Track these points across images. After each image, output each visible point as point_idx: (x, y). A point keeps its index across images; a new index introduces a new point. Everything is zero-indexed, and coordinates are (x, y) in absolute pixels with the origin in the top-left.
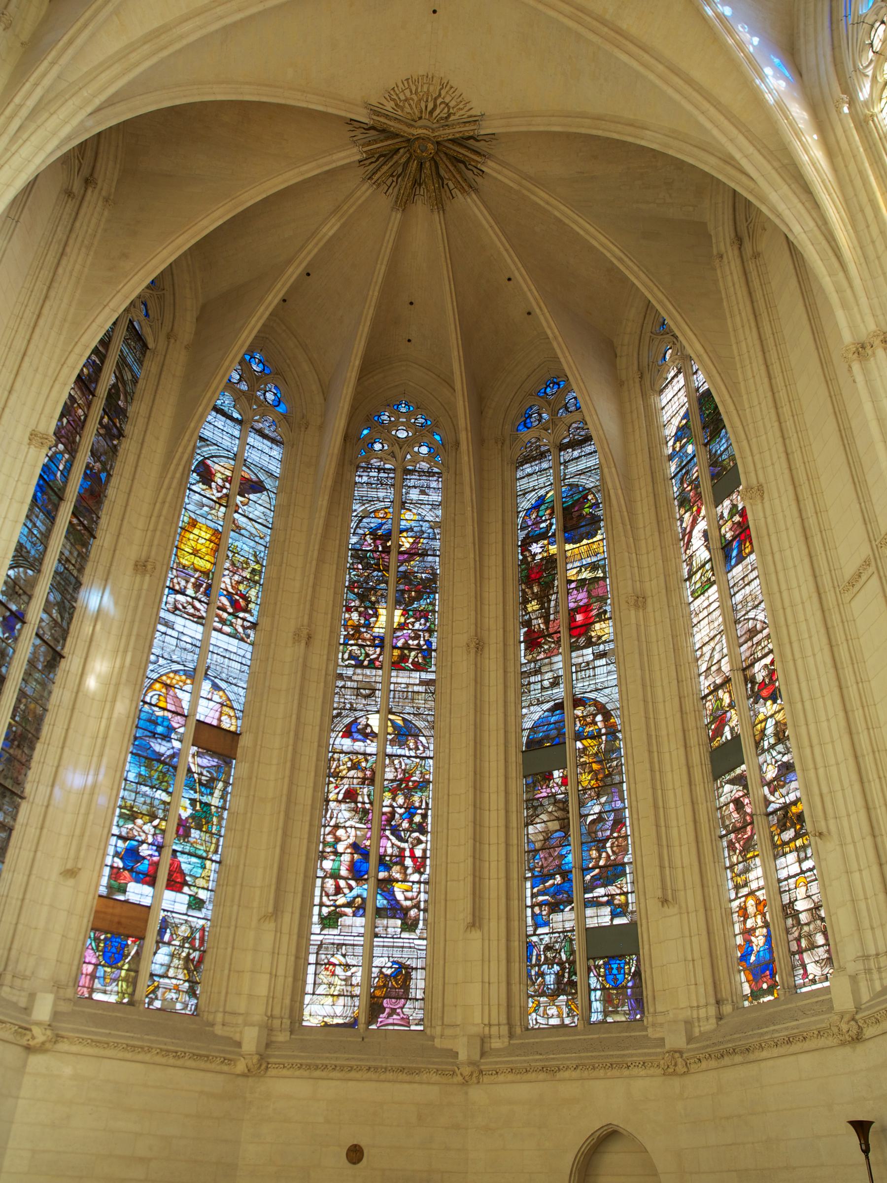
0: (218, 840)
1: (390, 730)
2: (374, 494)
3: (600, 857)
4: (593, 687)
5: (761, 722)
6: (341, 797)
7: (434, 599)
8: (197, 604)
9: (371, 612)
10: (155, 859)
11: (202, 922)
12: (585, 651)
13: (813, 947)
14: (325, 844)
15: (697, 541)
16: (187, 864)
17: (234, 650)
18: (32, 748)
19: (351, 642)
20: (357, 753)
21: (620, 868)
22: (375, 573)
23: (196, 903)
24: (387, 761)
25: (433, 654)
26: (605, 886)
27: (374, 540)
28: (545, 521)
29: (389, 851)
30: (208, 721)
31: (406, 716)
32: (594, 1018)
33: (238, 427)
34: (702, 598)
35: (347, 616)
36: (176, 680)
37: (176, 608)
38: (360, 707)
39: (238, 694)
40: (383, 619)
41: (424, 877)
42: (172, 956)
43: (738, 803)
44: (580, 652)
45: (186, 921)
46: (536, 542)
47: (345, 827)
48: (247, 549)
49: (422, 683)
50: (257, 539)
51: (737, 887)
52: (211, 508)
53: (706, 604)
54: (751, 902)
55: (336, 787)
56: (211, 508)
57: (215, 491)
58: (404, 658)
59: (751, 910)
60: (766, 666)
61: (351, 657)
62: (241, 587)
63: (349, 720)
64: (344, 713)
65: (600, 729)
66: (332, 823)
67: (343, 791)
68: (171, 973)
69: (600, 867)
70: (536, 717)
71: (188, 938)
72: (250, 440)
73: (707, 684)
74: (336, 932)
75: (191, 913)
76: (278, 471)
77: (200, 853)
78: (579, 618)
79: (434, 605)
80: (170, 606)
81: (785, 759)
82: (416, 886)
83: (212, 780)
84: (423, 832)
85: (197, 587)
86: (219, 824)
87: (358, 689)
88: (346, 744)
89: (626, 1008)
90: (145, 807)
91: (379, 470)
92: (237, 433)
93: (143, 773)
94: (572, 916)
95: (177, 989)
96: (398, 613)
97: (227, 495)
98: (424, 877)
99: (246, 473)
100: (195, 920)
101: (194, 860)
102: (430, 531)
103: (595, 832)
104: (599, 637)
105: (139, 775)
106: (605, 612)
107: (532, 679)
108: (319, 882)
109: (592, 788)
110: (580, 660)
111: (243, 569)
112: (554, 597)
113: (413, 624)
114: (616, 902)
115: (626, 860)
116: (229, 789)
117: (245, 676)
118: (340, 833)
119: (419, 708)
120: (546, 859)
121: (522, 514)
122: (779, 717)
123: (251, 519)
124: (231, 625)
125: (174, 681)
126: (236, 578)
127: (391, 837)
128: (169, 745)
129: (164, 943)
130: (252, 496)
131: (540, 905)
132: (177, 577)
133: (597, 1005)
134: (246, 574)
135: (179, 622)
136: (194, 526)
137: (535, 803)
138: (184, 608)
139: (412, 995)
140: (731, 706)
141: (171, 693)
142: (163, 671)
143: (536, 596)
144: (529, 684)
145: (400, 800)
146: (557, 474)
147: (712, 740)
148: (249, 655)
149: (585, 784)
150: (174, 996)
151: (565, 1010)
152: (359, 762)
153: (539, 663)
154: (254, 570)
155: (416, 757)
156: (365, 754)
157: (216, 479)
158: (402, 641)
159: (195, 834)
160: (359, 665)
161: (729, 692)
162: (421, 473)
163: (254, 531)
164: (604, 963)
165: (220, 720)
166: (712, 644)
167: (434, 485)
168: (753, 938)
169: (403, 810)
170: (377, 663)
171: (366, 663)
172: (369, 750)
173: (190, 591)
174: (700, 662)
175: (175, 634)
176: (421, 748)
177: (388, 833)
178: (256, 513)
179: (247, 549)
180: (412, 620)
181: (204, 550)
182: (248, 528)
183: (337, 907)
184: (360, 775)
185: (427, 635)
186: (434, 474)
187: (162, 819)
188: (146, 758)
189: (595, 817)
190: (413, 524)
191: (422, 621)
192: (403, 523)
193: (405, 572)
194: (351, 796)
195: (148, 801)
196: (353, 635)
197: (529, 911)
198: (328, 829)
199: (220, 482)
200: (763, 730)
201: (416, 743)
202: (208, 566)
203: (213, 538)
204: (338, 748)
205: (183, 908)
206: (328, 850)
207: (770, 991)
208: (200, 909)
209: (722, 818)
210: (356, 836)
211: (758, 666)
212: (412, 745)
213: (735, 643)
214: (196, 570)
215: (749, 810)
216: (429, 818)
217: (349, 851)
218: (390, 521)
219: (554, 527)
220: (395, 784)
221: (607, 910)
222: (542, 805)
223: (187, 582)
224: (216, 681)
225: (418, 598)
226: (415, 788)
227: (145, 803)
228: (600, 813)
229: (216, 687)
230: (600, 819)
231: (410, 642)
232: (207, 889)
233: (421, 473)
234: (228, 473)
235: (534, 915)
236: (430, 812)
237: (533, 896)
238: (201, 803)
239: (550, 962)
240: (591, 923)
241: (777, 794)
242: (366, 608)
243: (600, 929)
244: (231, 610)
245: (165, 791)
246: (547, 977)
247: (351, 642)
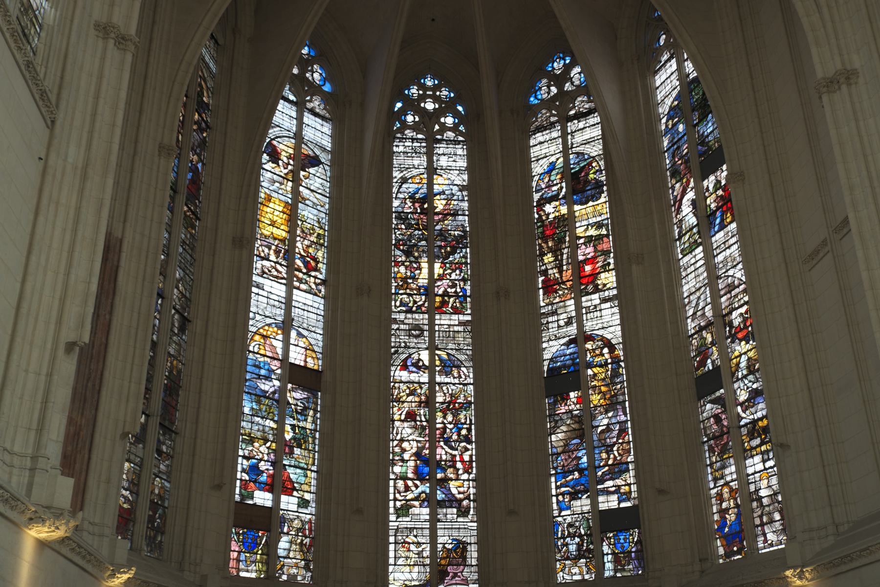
0: (314, 455)
1: (438, 363)
2: (409, 162)
3: (609, 458)
4: (600, 326)
5: (736, 357)
6: (403, 417)
7: (466, 253)
8: (278, 267)
9: (415, 265)
10: (271, 472)
11: (309, 517)
12: (594, 296)
13: (771, 521)
14: (393, 453)
15: (686, 208)
16: (294, 474)
17: (310, 303)
18: (178, 395)
19: (401, 292)
20: (413, 382)
21: (625, 466)
22: (416, 232)
24: (437, 388)
25: (468, 299)
26: (612, 479)
27: (413, 203)
28: (557, 184)
29: (444, 457)
30: (297, 362)
31: (450, 351)
32: (607, 574)
33: (294, 108)
34: (690, 256)
35: (396, 269)
36: (271, 331)
37: (264, 272)
38: (412, 345)
39: (317, 339)
40: (425, 272)
41: (472, 476)
42: (291, 542)
43: (717, 418)
44: (589, 297)
46: (550, 203)
47: (408, 441)
48: (312, 217)
49: (461, 324)
50: (319, 207)
51: (715, 480)
52: (281, 184)
53: (693, 261)
54: (726, 490)
55: (399, 409)
56: (281, 184)
57: (282, 168)
58: (444, 303)
59: (726, 496)
60: (741, 314)
61: (402, 304)
62: (311, 250)
63: (404, 356)
64: (400, 350)
65: (607, 360)
66: (398, 437)
67: (404, 413)
69: (609, 465)
70: (554, 350)
71: (300, 529)
72: (305, 120)
73: (693, 325)
74: (408, 519)
75: (300, 510)
76: (330, 145)
77: (302, 465)
78: (588, 268)
79: (466, 258)
80: (259, 271)
81: (755, 386)
82: (466, 483)
83: (305, 408)
84: (469, 442)
85: (277, 253)
86: (314, 443)
87: (410, 330)
88: (404, 375)
89: (631, 567)
90: (259, 433)
91: (413, 140)
92: (294, 114)
93: (255, 407)
94: (588, 502)
95: (297, 567)
96: (437, 266)
97: (291, 171)
98: (472, 476)
99: (305, 150)
101: (298, 471)
102: (459, 193)
103: (605, 439)
104: (605, 285)
105: (252, 409)
106: (609, 264)
107: (550, 319)
108: (392, 483)
109: (601, 405)
110: (589, 304)
111: (311, 234)
112: (565, 251)
113: (450, 275)
114: (622, 491)
115: (629, 460)
116: (318, 415)
117: (321, 325)
118: (405, 445)
119: (459, 344)
120: (566, 460)
121: (536, 178)
122: (751, 354)
123: (312, 191)
124: (306, 282)
125: (269, 333)
126: (306, 242)
127: (445, 447)
128: (271, 384)
130: (312, 170)
131: (563, 494)
132: (261, 245)
133: (609, 565)
134: (313, 238)
135: (267, 283)
136: (270, 201)
137: (557, 418)
138: (270, 271)
139: (469, 561)
140: (713, 344)
141: (268, 342)
142: (260, 325)
143: (551, 250)
144: (548, 323)
145: (450, 418)
146: (565, 143)
147: (697, 369)
148: (322, 307)
149: (595, 402)
150: (296, 571)
151: (585, 569)
152: (415, 390)
153: (555, 306)
154: (319, 235)
155: (460, 384)
156: (419, 383)
157: (282, 157)
158: (443, 289)
159: (297, 451)
160: (409, 311)
161: (712, 333)
162: (449, 142)
163: (315, 201)
164: (614, 536)
165: (305, 361)
166: (698, 294)
167: (460, 152)
168: (727, 516)
169: (452, 426)
170: (423, 309)
171: (414, 309)
172: (422, 380)
173: (273, 257)
174: (687, 308)
175: (265, 294)
176: (463, 377)
177: (442, 444)
178: (317, 185)
179: (312, 217)
180: (449, 271)
181: (279, 221)
182: (311, 198)
183: (407, 501)
184: (417, 399)
185: (462, 284)
186: (459, 142)
187: (272, 442)
188: (256, 395)
189: (604, 427)
190: (445, 188)
191: (458, 272)
192: (436, 187)
193: (441, 230)
194: (411, 416)
195: (261, 428)
196: (402, 286)
197: (554, 499)
198: (395, 443)
199: (285, 160)
200: (738, 364)
201: (459, 372)
202: (284, 234)
203: (285, 210)
204: (398, 378)
205: (295, 508)
206: (397, 458)
207: (738, 552)
208: (306, 508)
209: (705, 428)
210: (418, 447)
211: (735, 314)
212: (456, 375)
213: (716, 296)
214: (275, 239)
215: (725, 423)
216: (473, 431)
217: (413, 458)
218: (425, 186)
219: (564, 190)
220: (445, 406)
221: (615, 497)
222: (561, 419)
223: (270, 249)
224: (300, 330)
225: (453, 252)
226: (461, 408)
227: (258, 430)
228: (608, 425)
229: (300, 335)
230: (608, 429)
231: (449, 290)
232: (310, 492)
233: (449, 142)
234: (291, 151)
235: (558, 502)
236: (473, 427)
237: (557, 487)
238: (299, 427)
239: (572, 536)
240: (603, 507)
241: (748, 412)
242: (411, 262)
243: (610, 511)
244: (304, 271)
245: (272, 420)
246: (570, 547)
247: (401, 292)
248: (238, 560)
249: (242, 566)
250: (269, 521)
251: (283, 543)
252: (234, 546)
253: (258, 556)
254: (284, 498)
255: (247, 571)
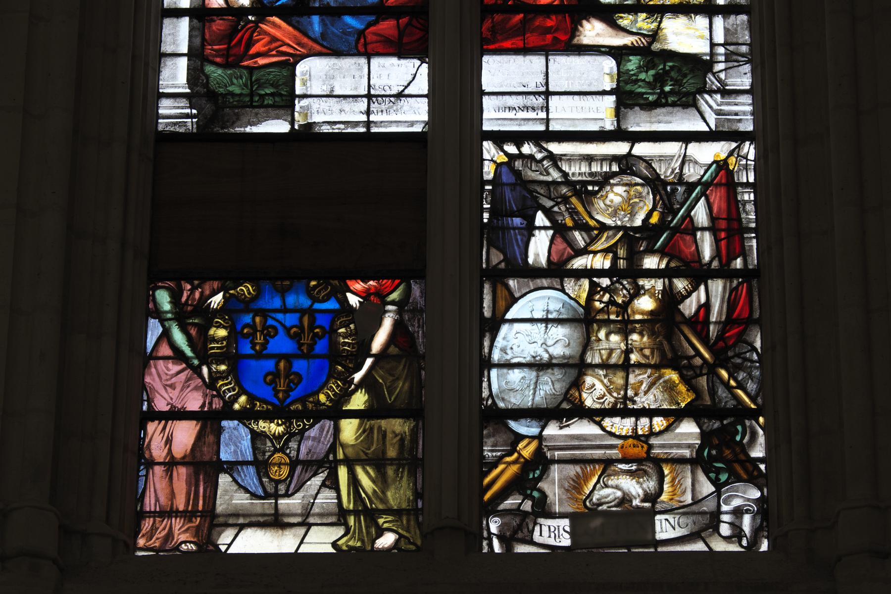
11: (707, 153)
23: (659, 80)
42: (585, 320)
45: (627, 164)
68: (595, 391)
75: (639, 122)
95: (645, 459)
100: (672, 148)
129: (533, 273)
248: (205, 466)
249: (230, 495)
250: (433, 220)
251: (530, 333)
252: (170, 386)
253: (349, 429)
254: (500, 72)
255: (276, 522)
